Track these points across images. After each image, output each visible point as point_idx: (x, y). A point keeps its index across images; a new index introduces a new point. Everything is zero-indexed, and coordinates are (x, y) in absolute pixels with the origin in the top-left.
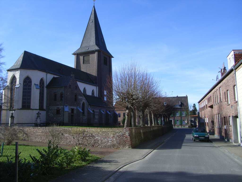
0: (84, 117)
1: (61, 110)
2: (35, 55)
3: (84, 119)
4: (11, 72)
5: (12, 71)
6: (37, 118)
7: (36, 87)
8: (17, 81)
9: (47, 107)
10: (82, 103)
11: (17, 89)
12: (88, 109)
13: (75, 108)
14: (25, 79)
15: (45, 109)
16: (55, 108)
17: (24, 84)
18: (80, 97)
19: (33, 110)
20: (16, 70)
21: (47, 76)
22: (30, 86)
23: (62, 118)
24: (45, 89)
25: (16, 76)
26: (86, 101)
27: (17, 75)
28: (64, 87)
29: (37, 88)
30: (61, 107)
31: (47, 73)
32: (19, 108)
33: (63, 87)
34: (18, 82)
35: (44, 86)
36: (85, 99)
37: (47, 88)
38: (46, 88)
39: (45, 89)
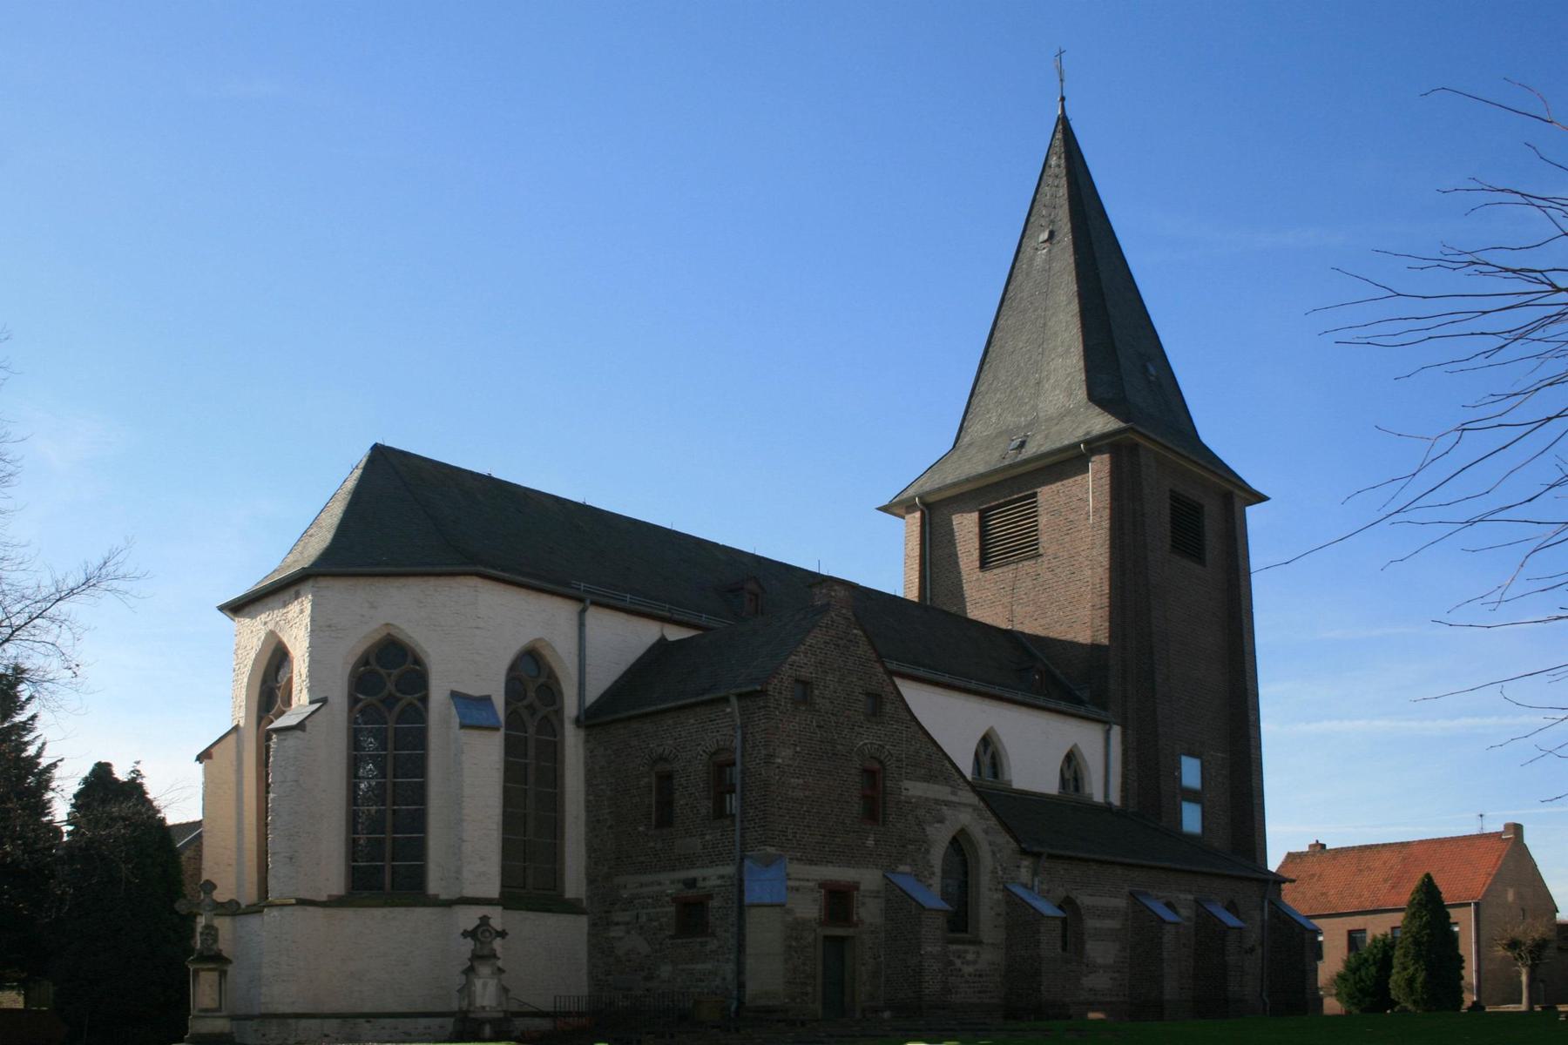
0: (970, 957)
1: (714, 904)
2: (489, 479)
3: (968, 969)
4: (253, 617)
5: (258, 606)
6: (470, 971)
7: (462, 716)
8: (296, 679)
9: (591, 881)
10: (940, 837)
11: (292, 741)
12: (1006, 889)
13: (868, 878)
14: (364, 660)
15: (579, 900)
16: (669, 883)
17: (353, 701)
18: (915, 789)
19: (449, 904)
20: (286, 596)
21: (582, 625)
22: (418, 713)
23: (729, 969)
24: (573, 743)
25: (285, 640)
26: (993, 822)
27: (295, 631)
28: (740, 696)
29: (468, 722)
30: (722, 877)
31: (580, 600)
32: (324, 898)
33: (726, 700)
34: (301, 700)
35: (559, 712)
36: (975, 808)
37: (587, 727)
38: (582, 733)
39: (573, 743)
